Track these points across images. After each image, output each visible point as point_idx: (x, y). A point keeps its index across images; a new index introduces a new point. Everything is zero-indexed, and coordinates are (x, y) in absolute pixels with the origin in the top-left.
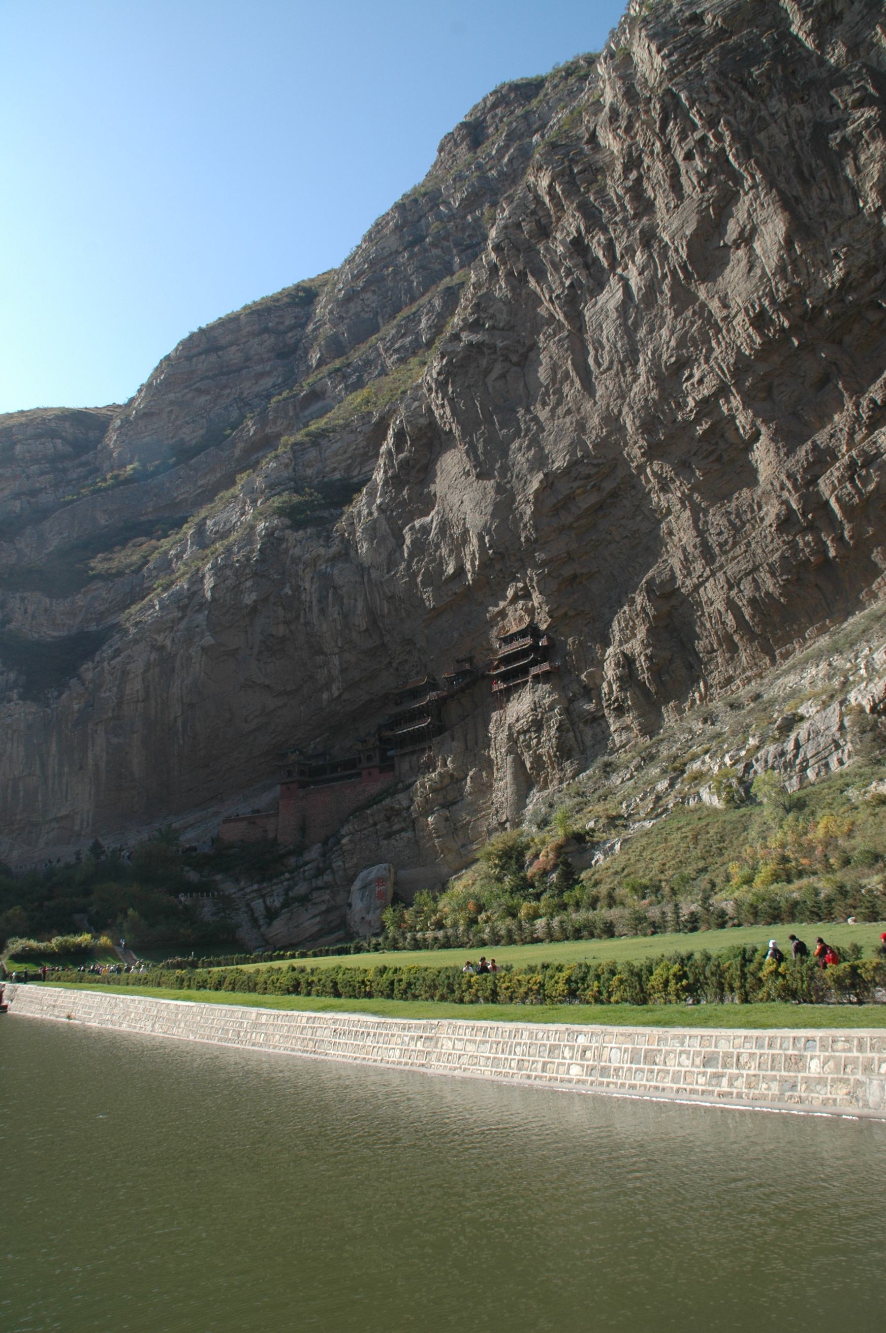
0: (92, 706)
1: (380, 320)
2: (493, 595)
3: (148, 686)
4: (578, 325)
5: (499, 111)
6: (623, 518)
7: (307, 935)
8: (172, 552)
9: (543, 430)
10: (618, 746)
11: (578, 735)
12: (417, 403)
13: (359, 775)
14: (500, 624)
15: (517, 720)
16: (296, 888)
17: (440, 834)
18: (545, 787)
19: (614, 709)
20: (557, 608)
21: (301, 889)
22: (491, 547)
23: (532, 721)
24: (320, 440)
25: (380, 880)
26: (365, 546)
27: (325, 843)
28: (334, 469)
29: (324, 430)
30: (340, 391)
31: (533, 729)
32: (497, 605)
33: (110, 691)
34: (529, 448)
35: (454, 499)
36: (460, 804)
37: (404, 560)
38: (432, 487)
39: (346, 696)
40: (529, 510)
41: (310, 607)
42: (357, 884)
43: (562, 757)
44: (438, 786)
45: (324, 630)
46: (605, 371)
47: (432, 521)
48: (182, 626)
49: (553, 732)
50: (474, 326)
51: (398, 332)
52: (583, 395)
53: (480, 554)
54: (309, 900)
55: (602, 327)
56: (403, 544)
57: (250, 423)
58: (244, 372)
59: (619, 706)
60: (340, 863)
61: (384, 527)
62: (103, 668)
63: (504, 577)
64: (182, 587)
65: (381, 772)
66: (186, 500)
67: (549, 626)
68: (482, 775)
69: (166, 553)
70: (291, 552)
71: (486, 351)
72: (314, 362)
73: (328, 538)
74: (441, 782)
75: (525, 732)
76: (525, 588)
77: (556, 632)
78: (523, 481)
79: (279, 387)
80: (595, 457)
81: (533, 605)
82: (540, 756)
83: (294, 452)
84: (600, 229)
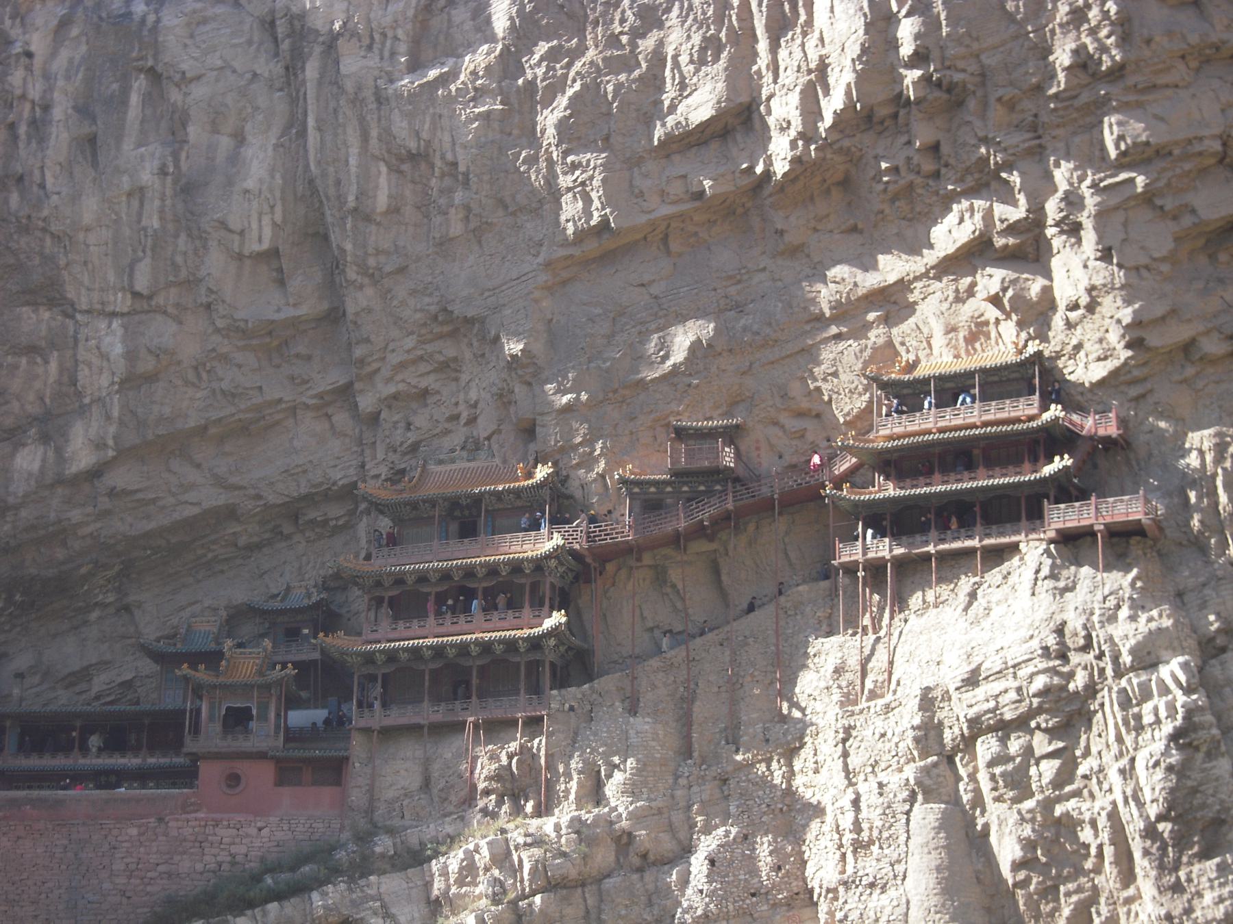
2: (854, 229)
13: (186, 776)
14: (876, 336)
15: (972, 680)
20: (1163, 318)
22: (919, 58)
23: (1044, 693)
31: (1041, 719)
32: (869, 265)
37: (492, 39)
39: (120, 478)
41: (39, 127)
43: (1181, 842)
44: (573, 873)
45: (87, 218)
49: (1154, 744)
53: (861, 78)
63: (936, 175)
65: (280, 782)
67: (1115, 374)
68: (753, 859)
74: (585, 857)
75: (1004, 729)
76: (1034, 225)
81: (1047, 291)
82: (1069, 825)
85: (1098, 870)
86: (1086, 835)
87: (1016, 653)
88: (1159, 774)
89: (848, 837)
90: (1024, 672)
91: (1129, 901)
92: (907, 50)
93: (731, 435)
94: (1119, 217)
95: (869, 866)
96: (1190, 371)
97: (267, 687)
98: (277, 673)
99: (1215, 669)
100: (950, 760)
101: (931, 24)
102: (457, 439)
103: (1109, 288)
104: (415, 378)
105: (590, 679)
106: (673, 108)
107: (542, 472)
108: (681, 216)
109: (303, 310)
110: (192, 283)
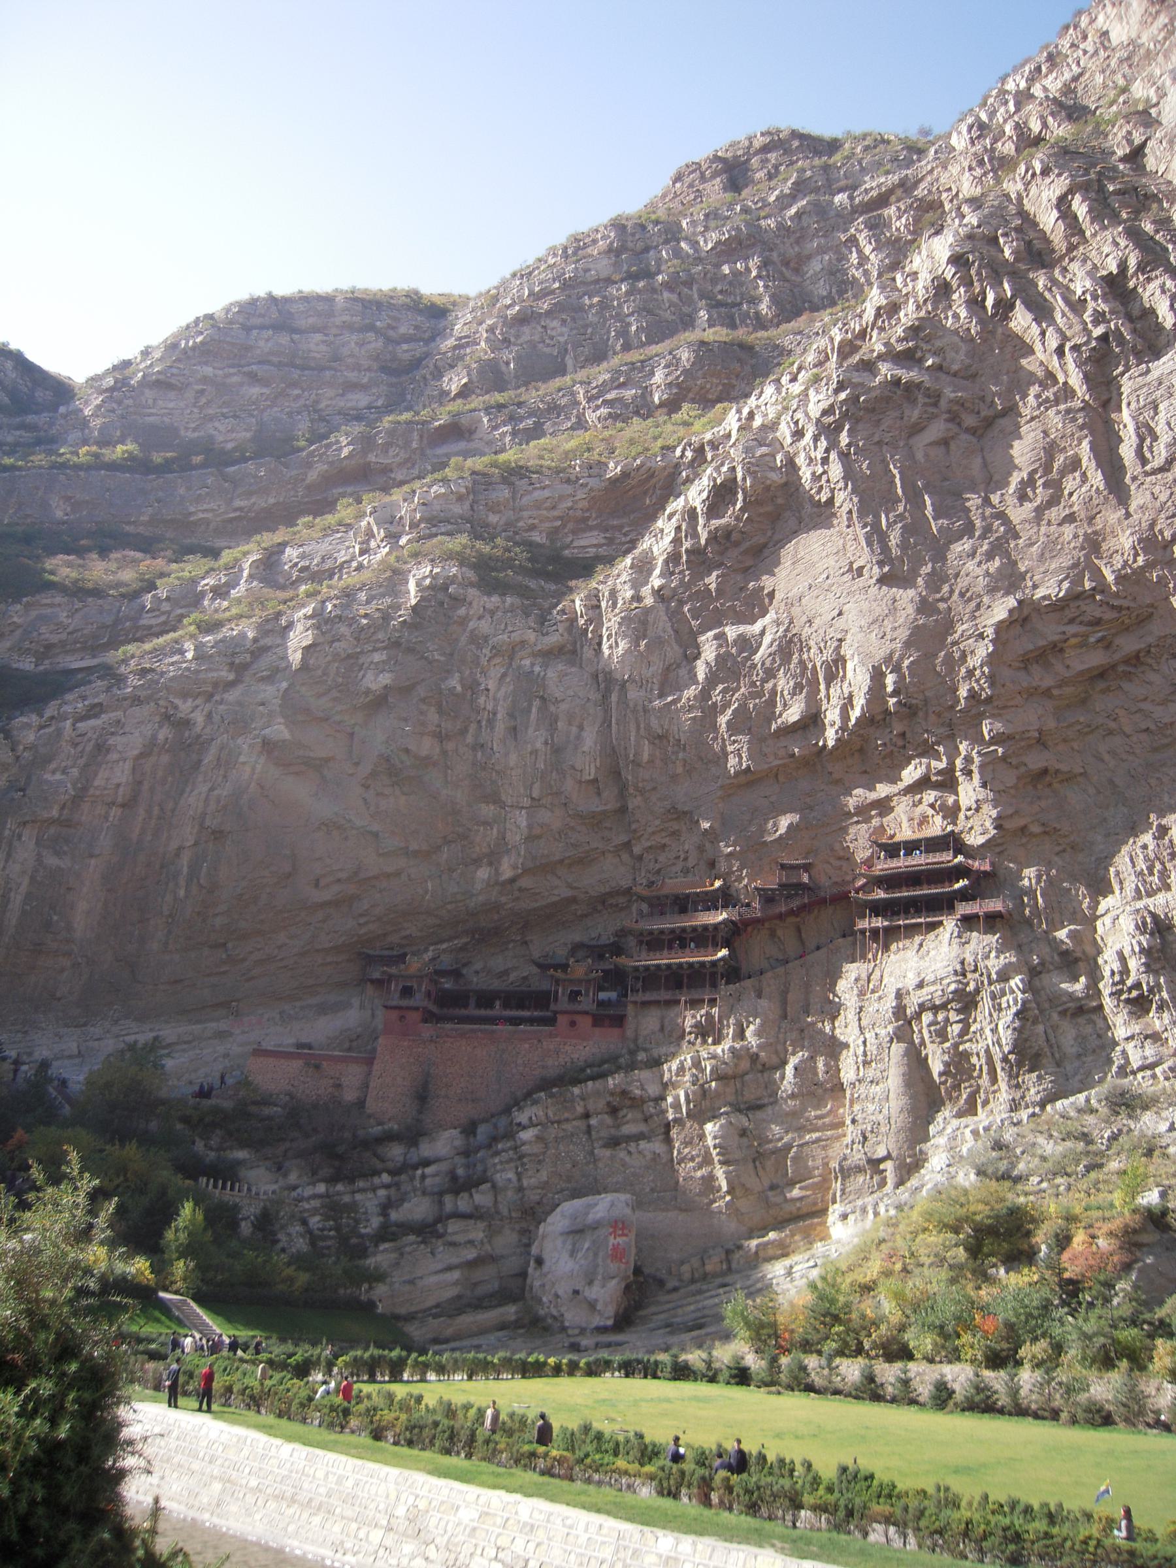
0: (23, 790)
1: (569, 361)
2: (865, 772)
3: (140, 783)
4: (1104, 397)
5: (773, 157)
6: (1145, 699)
7: (430, 1303)
8: (210, 581)
9: (1017, 536)
10: (1135, 1065)
11: (1050, 1031)
12: (764, 450)
13: (551, 1021)
14: (875, 822)
15: (920, 985)
16: (406, 1205)
17: (731, 1157)
18: (970, 1109)
19: (1128, 1001)
21: (417, 1209)
22: (896, 693)
23: (955, 992)
24: (513, 479)
25: (618, 1225)
26: (623, 645)
27: (470, 1129)
28: (533, 528)
29: (521, 467)
30: (504, 434)
31: (953, 1005)
33: (64, 772)
34: (990, 556)
35: (824, 608)
36: (769, 1110)
37: (697, 683)
38: (767, 582)
39: (525, 882)
40: (983, 650)
41: (491, 722)
42: (557, 1222)
43: (1020, 1064)
44: (730, 1072)
45: (512, 764)
46: (1154, 472)
47: (763, 633)
48: (233, 695)
49: (1007, 1017)
50: (907, 358)
51: (613, 380)
52: (1106, 499)
53: (868, 701)
54: (440, 1236)
55: (1156, 408)
56: (698, 656)
57: (344, 441)
58: (328, 374)
59: (1141, 996)
60: (511, 1175)
61: (662, 624)
62: (59, 733)
63: (904, 747)
64: (242, 635)
65: (595, 1025)
66: (207, 522)
67: (989, 841)
68: (815, 1068)
69: (194, 581)
70: (472, 625)
71: (921, 400)
72: (454, 388)
73: (543, 620)
74: (736, 1065)
75: (935, 1009)
76: (950, 770)
77: (1000, 853)
78: (973, 604)
79: (389, 409)
80: (1116, 595)
81: (957, 802)
82: (966, 1055)
83: (475, 482)
84: (1166, 271)
85: (980, 1077)
86: (974, 1060)
87: (941, 973)
88: (1010, 1032)
89: (860, 1059)
90: (945, 982)
91: (994, 1092)
92: (890, 689)
93: (807, 868)
94: (991, 767)
95: (871, 1073)
96: (1024, 840)
97: (588, 981)
98: (594, 975)
99: (1037, 982)
100: (910, 1023)
101: (902, 677)
102: (678, 868)
103: (986, 801)
104: (659, 839)
105: (739, 980)
106: (780, 715)
107: (718, 884)
108: (784, 765)
109: (608, 807)
110: (558, 794)
